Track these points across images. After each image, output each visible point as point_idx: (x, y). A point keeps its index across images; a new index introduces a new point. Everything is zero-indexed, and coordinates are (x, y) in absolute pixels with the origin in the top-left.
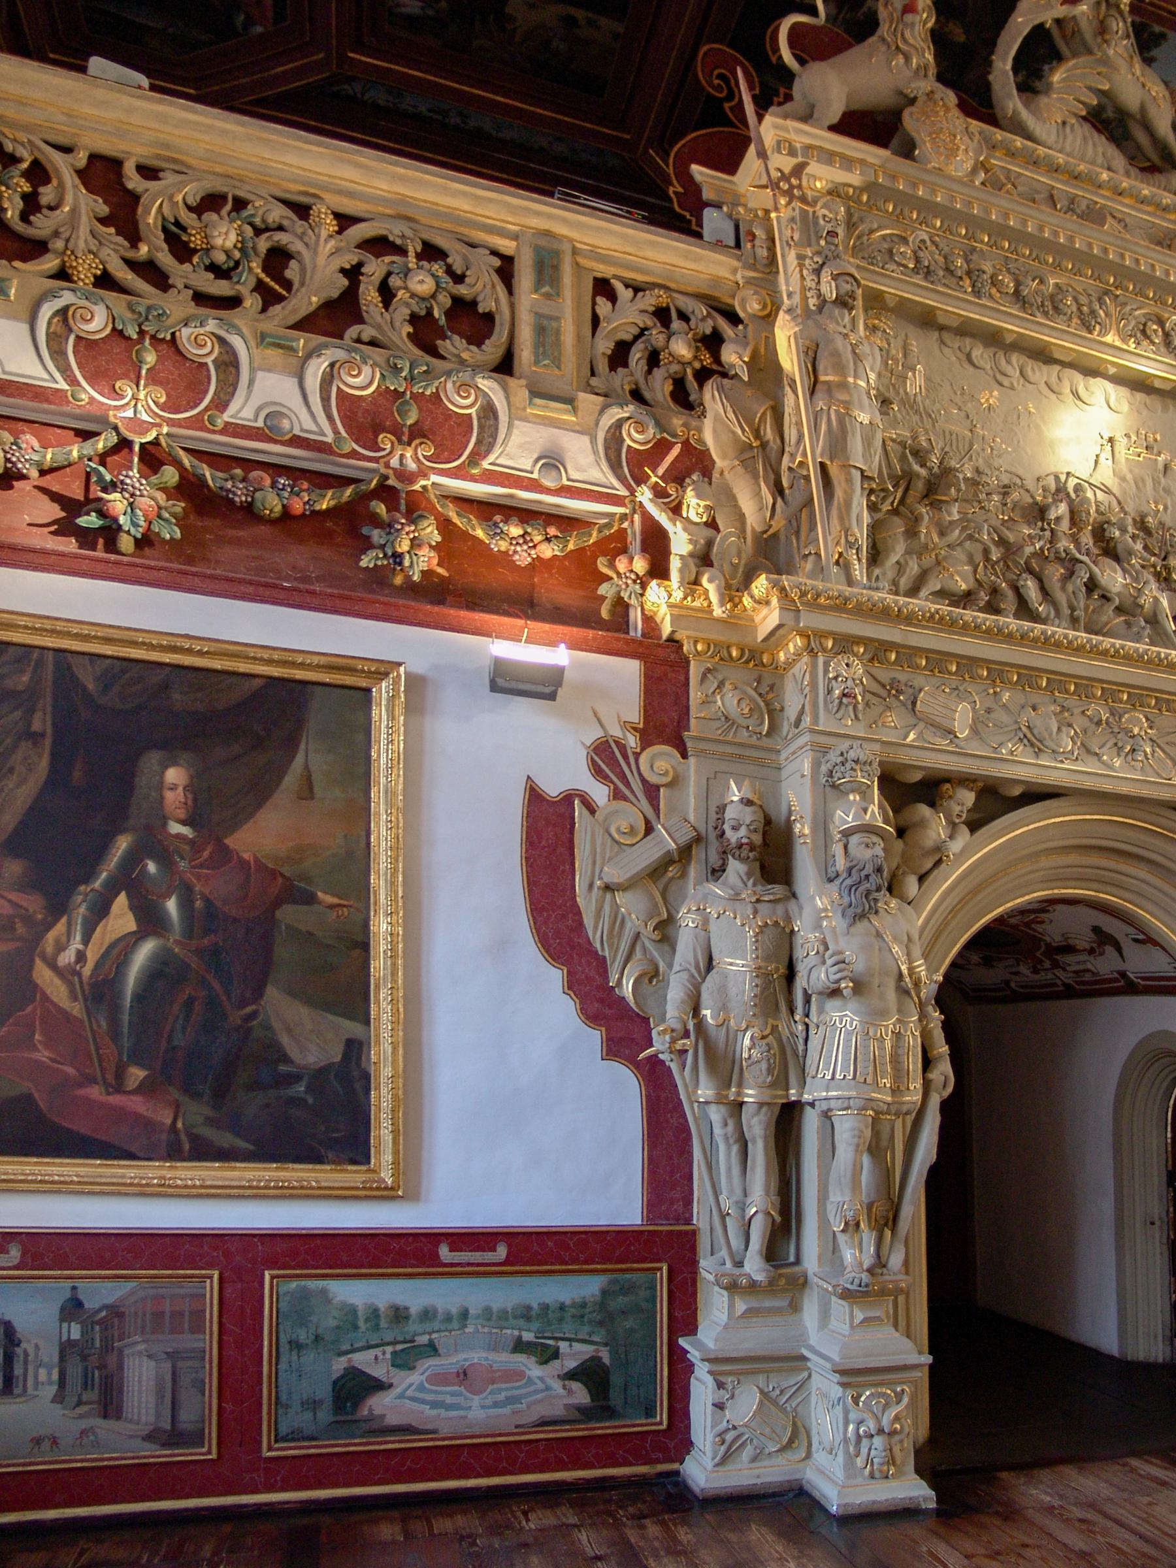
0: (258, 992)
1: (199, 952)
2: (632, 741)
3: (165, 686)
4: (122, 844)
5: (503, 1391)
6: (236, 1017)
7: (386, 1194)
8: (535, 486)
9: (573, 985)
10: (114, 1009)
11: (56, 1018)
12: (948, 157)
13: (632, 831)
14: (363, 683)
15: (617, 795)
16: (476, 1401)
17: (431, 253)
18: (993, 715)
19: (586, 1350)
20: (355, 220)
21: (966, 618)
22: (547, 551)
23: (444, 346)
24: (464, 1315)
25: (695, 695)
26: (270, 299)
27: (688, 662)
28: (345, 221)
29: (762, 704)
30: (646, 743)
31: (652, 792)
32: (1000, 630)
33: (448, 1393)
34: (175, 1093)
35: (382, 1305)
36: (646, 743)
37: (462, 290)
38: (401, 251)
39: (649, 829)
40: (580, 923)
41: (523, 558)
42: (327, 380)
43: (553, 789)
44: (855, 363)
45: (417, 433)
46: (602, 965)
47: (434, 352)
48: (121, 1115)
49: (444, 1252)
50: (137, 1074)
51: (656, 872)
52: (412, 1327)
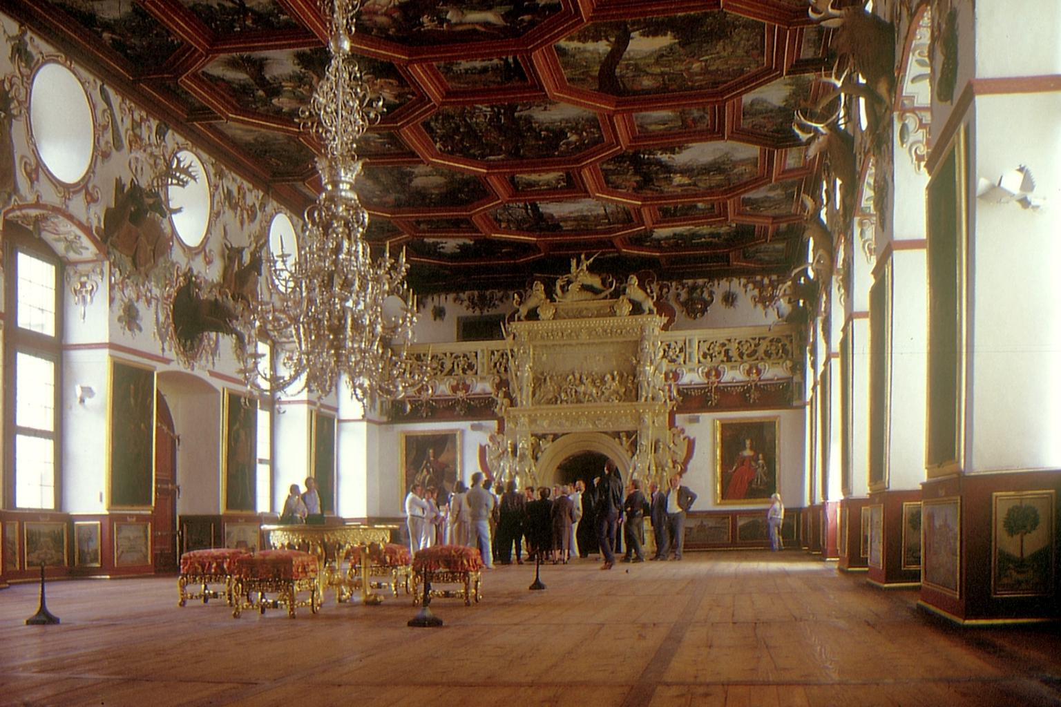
0: (442, 481)
4: (425, 462)
31: (499, 443)
36: (498, 433)
43: (483, 444)
51: (499, 456)
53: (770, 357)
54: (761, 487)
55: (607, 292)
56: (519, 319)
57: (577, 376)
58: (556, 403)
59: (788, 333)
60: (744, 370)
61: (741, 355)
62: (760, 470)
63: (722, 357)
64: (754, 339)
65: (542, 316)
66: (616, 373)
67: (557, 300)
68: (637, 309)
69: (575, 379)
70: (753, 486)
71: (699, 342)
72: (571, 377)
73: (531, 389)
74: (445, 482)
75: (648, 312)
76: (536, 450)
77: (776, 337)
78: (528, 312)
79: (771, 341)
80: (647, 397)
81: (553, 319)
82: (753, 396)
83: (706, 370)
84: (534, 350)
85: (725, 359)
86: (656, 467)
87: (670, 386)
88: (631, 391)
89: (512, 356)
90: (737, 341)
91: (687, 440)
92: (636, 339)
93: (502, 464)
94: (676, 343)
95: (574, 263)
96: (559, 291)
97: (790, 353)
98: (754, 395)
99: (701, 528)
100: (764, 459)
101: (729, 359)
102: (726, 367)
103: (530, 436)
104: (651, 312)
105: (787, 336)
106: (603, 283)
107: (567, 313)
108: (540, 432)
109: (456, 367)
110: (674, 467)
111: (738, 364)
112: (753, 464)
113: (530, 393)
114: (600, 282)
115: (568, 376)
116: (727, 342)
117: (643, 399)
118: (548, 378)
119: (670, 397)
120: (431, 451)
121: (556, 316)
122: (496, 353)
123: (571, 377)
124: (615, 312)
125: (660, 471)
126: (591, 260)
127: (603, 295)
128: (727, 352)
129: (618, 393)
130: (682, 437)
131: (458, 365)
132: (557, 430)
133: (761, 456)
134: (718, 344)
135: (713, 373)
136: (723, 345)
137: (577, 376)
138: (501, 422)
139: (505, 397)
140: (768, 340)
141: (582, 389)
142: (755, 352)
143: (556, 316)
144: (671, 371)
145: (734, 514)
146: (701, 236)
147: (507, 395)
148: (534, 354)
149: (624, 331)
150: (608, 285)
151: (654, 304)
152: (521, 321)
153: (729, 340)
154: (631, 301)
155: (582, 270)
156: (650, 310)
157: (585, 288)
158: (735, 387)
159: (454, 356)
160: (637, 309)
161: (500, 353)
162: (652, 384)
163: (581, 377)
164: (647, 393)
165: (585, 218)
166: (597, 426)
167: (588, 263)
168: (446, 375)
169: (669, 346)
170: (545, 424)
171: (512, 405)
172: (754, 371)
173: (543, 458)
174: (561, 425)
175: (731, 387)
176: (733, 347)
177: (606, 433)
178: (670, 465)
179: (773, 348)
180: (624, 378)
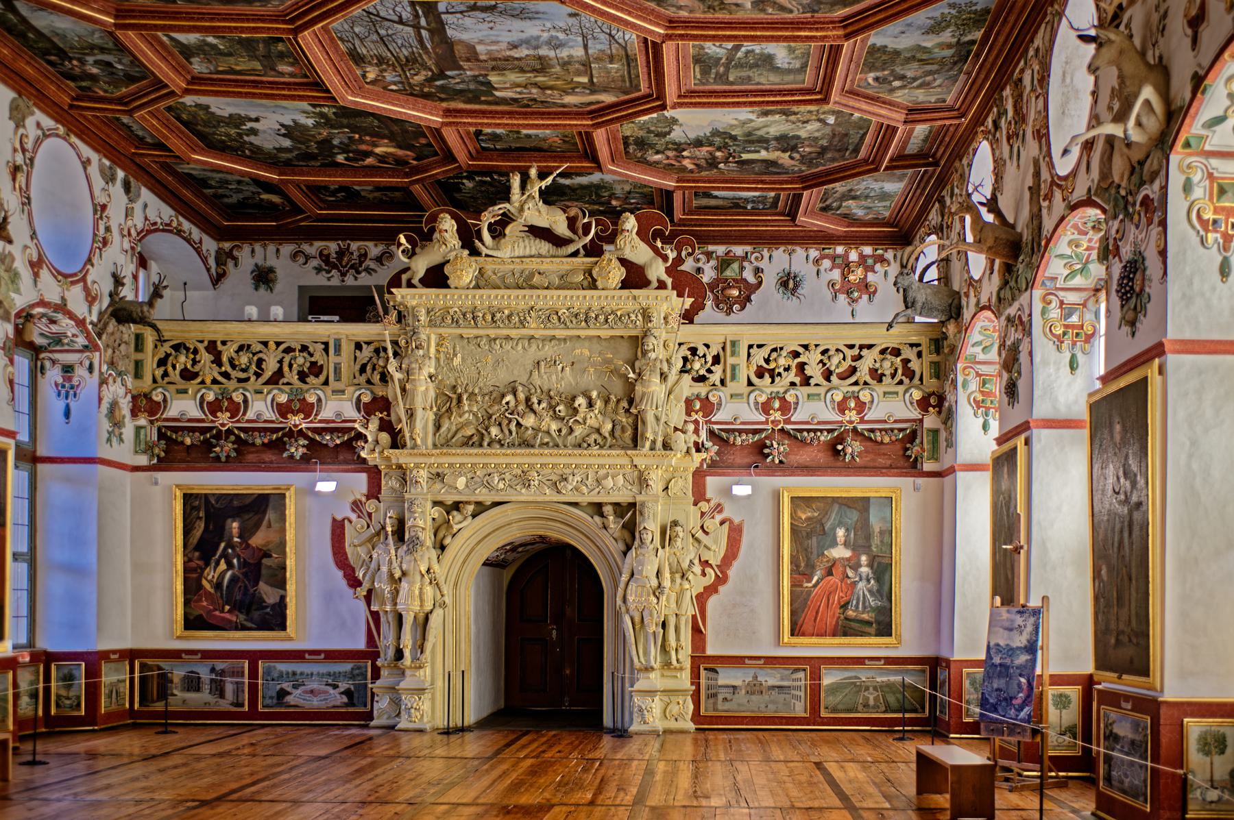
1: (243, 574)
2: (364, 499)
3: (231, 500)
5: (323, 697)
6: (252, 591)
7: (290, 639)
8: (333, 422)
9: (345, 576)
10: (222, 590)
11: (208, 594)
13: (363, 527)
14: (283, 492)
15: (359, 517)
16: (315, 699)
17: (304, 348)
19: (348, 686)
20: (282, 343)
22: (338, 442)
23: (308, 380)
24: (312, 674)
25: (383, 482)
26: (258, 375)
28: (278, 344)
30: (368, 499)
31: (370, 515)
33: (307, 696)
34: (237, 612)
35: (290, 670)
36: (368, 499)
37: (313, 359)
38: (294, 350)
39: (368, 527)
40: (347, 558)
41: (331, 445)
42: (273, 400)
43: (339, 518)
45: (299, 411)
46: (353, 570)
47: (305, 383)
48: (223, 619)
49: (307, 656)
50: (227, 608)
51: (370, 540)
52: (297, 677)
53: (880, 381)
54: (865, 616)
55: (579, 245)
56: (410, 285)
57: (521, 396)
58: (481, 445)
59: (914, 339)
60: (833, 400)
61: (828, 375)
62: (861, 585)
63: (792, 376)
64: (851, 347)
66: (594, 394)
67: (484, 251)
68: (635, 278)
69: (516, 400)
70: (850, 613)
71: (750, 347)
72: (509, 398)
73: (432, 417)
74: (262, 585)
75: (655, 284)
76: (440, 535)
77: (891, 345)
79: (883, 352)
80: (654, 442)
82: (849, 450)
83: (763, 399)
84: (438, 345)
85: (797, 380)
86: (672, 573)
87: (696, 422)
88: (623, 430)
89: (396, 354)
90: (821, 349)
91: (727, 525)
92: (634, 333)
93: (375, 556)
94: (707, 346)
95: (516, 181)
96: (486, 235)
97: (917, 376)
98: (853, 447)
99: (755, 688)
100: (870, 565)
101: (806, 381)
102: (803, 391)
103: (429, 504)
104: (662, 285)
105: (912, 345)
106: (572, 223)
107: (503, 277)
108: (450, 499)
109: (286, 369)
110: (704, 574)
111: (821, 390)
112: (850, 573)
114: (566, 223)
115: (503, 396)
116: (801, 350)
117: (648, 444)
118: (465, 397)
119: (696, 444)
120: (235, 525)
121: (481, 282)
122: (364, 346)
123: (509, 398)
124: (594, 281)
125: (678, 580)
126: (549, 180)
127: (571, 249)
128: (801, 367)
129: (598, 431)
130: (719, 518)
131: (290, 366)
132: (487, 498)
133: (864, 558)
134: (784, 353)
135: (777, 405)
136: (796, 355)
137: (521, 396)
138: (375, 475)
140: (876, 350)
141: (529, 421)
142: (853, 370)
143: (481, 282)
144: (698, 397)
145: (815, 666)
146: (763, 142)
147: (386, 426)
148: (438, 351)
149: (611, 317)
150: (580, 231)
151: (668, 271)
152: (414, 286)
153: (806, 347)
154: (623, 262)
155: (531, 197)
156: (659, 281)
157: (536, 232)
158: (815, 431)
159: (282, 347)
160: (635, 278)
161: (372, 348)
162: (663, 420)
163: (528, 400)
164: (655, 433)
165: (542, 66)
166: (559, 492)
167: (544, 184)
168: (266, 383)
169: (694, 351)
170: (461, 482)
171: (394, 445)
172: (853, 405)
173: (456, 547)
174: (489, 486)
175: (809, 431)
176: (812, 359)
177: (575, 505)
178: (697, 569)
179: (887, 364)
180: (612, 405)
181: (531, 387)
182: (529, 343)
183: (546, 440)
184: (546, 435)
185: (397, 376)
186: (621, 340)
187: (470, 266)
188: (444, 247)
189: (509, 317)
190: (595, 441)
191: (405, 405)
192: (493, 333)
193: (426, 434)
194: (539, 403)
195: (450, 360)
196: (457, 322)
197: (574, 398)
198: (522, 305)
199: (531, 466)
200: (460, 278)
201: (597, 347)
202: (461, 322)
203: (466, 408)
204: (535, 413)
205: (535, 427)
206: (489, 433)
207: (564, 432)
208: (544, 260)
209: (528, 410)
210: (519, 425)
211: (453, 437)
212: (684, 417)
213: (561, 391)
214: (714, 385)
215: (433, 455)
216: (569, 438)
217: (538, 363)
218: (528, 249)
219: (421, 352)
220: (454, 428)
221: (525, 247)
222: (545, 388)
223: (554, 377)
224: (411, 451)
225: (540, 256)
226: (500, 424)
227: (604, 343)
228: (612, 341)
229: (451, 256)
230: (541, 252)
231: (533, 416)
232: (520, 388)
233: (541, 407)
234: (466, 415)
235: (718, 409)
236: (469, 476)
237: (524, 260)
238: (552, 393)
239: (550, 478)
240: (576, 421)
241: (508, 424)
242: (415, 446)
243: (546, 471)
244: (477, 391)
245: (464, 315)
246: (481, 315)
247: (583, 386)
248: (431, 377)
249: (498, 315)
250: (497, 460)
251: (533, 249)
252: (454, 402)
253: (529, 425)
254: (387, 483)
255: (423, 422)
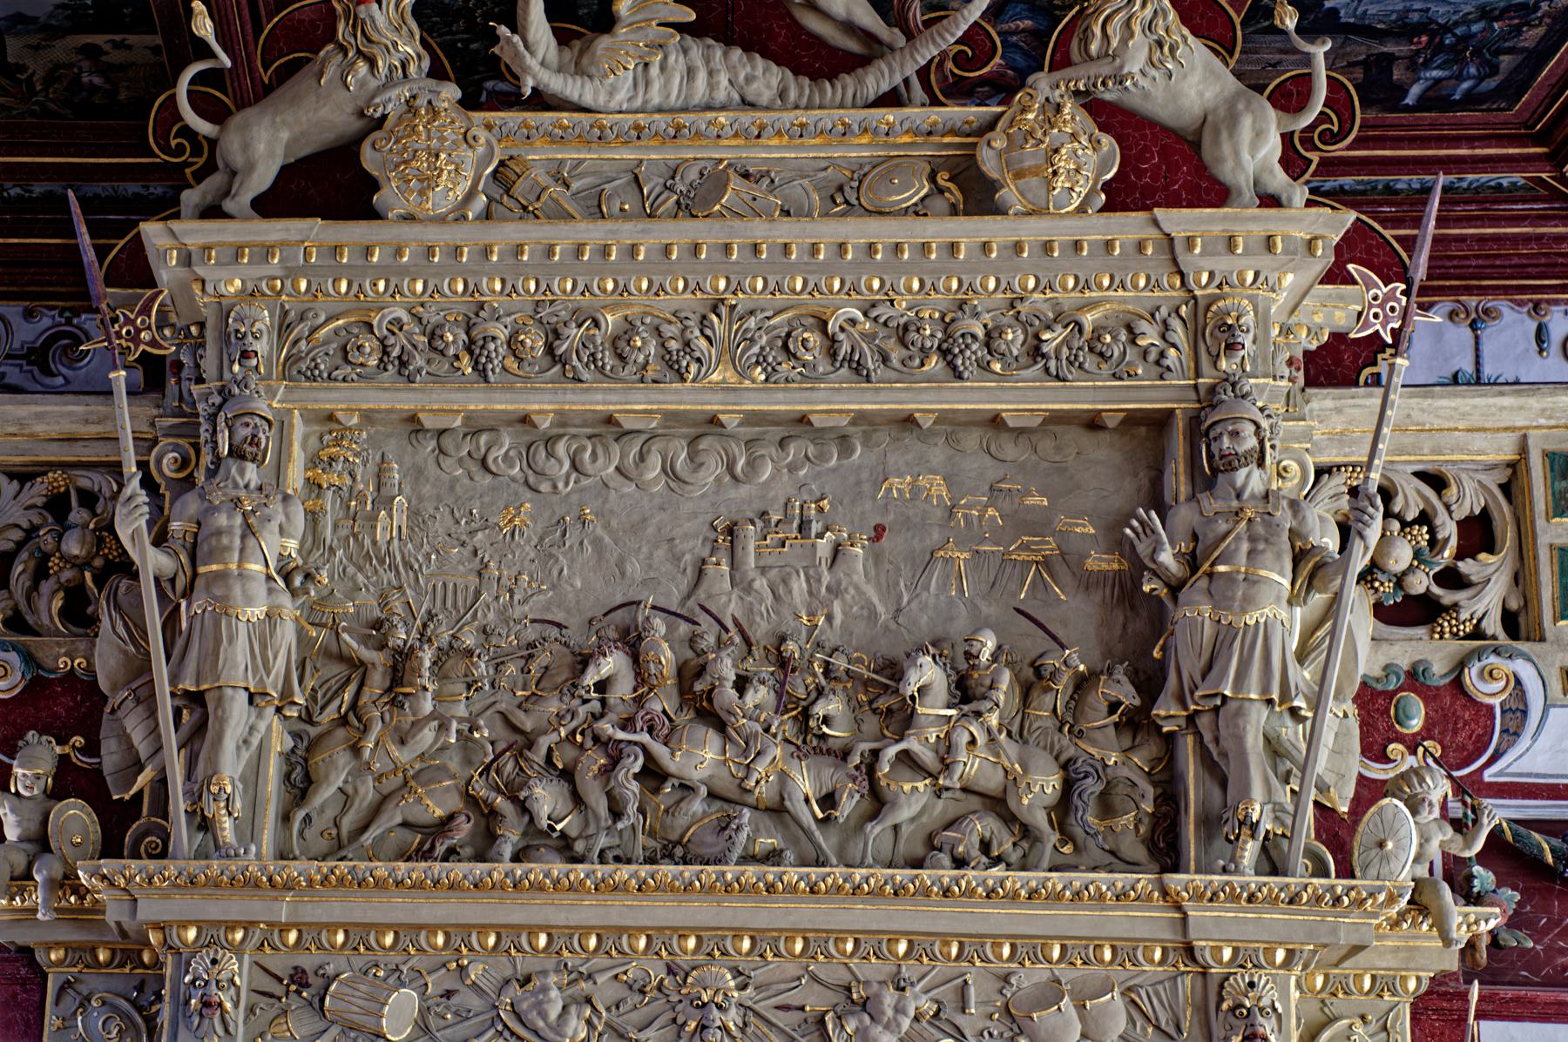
12: (421, 193)
18: (455, 1000)
21: (378, 873)
25: (51, 1020)
27: (45, 976)
29: (139, 1020)
32: (436, 882)
44: (243, 537)
56: (212, 212)
57: (666, 657)
65: (390, 197)
72: (612, 664)
73: (280, 742)
78: (285, 171)
81: (487, 215)
113: (273, 769)
115: (583, 661)
118: (427, 656)
127: (877, 80)
137: (666, 657)
139: (57, 793)
144: (1415, 678)
163: (691, 674)
181: (703, 619)
182: (692, 456)
183: (767, 842)
184: (766, 821)
185: (153, 562)
186: (1087, 439)
187: (467, 139)
188: (362, 67)
189: (620, 343)
190: (985, 846)
191: (174, 679)
192: (543, 404)
193: (254, 806)
194: (742, 684)
195: (358, 519)
196: (403, 364)
197: (894, 670)
198: (679, 296)
199: (714, 942)
200: (427, 183)
201: (976, 466)
202: (419, 361)
203: (427, 706)
204: (721, 727)
205: (726, 786)
206: (523, 808)
207: (848, 805)
208: (765, 117)
209: (687, 715)
210: (653, 775)
211: (364, 828)
212: (1355, 765)
213: (832, 638)
214: (1477, 634)
215: (289, 886)
216: (875, 830)
217: (730, 531)
218: (701, 77)
219: (252, 473)
220: (367, 792)
221: (691, 72)
222: (761, 631)
223: (799, 585)
224: (194, 866)
225: (747, 104)
226: (568, 775)
227: (1010, 450)
228: (1046, 445)
229: (392, 102)
230: (752, 91)
231: (713, 737)
232: (659, 624)
233: (751, 698)
234: (427, 735)
235: (1513, 734)
236: (434, 983)
237: (683, 118)
238: (791, 646)
239: (792, 998)
240: (906, 758)
241: (607, 771)
242: (211, 846)
243: (775, 969)
244: (469, 641)
245: (434, 335)
246: (502, 334)
247: (924, 622)
248: (287, 578)
249: (574, 334)
250: (561, 912)
251: (723, 80)
252: (377, 681)
253: (696, 775)
254: (67, 1023)
255: (246, 755)
